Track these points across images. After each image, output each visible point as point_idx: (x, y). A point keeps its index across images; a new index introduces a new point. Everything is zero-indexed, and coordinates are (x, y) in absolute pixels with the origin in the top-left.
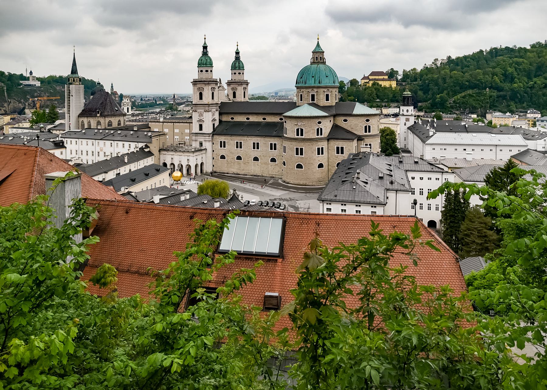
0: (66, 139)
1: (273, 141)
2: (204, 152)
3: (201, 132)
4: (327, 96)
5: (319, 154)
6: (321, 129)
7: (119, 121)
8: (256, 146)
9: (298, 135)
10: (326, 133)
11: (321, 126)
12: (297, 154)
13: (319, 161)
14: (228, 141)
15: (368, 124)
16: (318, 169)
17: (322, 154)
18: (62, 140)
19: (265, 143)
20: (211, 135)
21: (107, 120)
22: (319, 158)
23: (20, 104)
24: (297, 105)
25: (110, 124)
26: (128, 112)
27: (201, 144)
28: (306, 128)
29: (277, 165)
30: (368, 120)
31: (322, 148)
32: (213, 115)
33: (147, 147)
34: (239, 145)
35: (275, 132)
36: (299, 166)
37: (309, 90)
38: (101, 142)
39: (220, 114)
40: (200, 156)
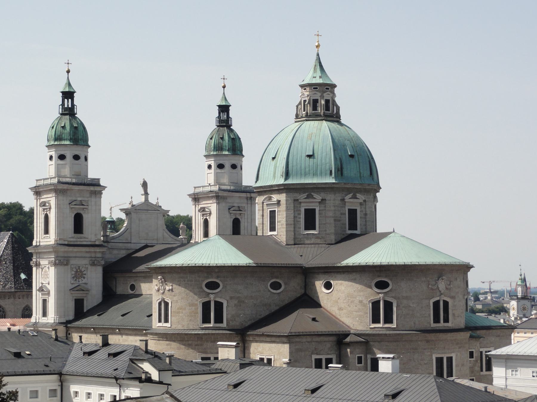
4: (310, 215)
28: (175, 298)
32: (79, 274)
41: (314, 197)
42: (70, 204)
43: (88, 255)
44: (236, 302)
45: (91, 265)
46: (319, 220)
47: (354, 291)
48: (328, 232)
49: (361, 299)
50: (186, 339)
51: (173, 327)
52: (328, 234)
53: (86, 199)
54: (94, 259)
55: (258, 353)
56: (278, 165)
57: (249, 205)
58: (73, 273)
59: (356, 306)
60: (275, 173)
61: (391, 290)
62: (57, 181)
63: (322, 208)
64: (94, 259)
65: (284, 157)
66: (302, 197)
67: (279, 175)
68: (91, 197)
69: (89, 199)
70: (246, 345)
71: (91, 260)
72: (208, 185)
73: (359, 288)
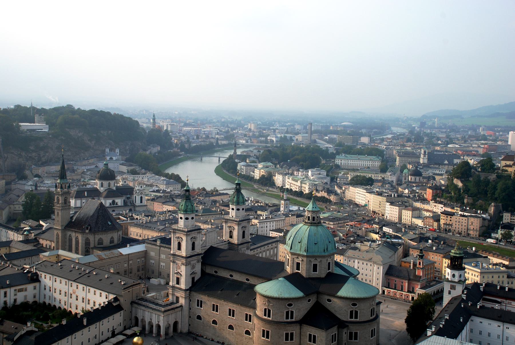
0: (41, 273)
2: (180, 309)
3: (177, 286)
5: (287, 339)
6: (292, 312)
7: (112, 238)
8: (232, 313)
9: (265, 315)
10: (298, 315)
11: (290, 309)
12: (263, 336)
15: (354, 308)
17: (292, 339)
18: (36, 273)
19: (241, 311)
20: (188, 291)
21: (98, 237)
23: (21, 160)
25: (100, 242)
26: (141, 202)
30: (354, 305)
31: (292, 334)
32: (193, 267)
33: (116, 299)
34: (215, 308)
35: (253, 301)
38: (75, 284)
39: (203, 264)
40: (173, 315)
42: (191, 239)
44: (298, 310)
45: (197, 262)
51: (273, 320)
56: (302, 246)
60: (301, 249)
61: (358, 307)
63: (320, 264)
66: (312, 260)
67: (303, 250)
68: (198, 234)
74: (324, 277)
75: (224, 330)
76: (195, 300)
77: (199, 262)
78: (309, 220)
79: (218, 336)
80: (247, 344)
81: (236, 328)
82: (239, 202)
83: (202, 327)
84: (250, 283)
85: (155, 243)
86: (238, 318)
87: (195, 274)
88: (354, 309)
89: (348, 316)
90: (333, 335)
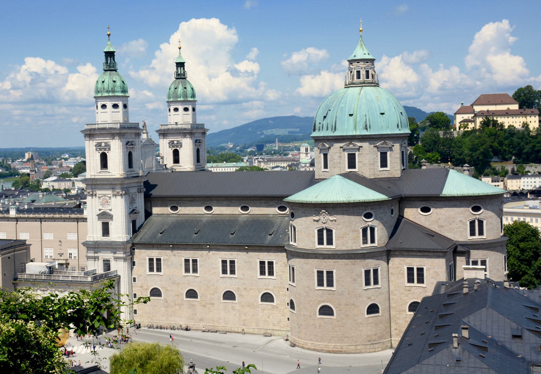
1: (266, 257)
3: (106, 239)
5: (368, 283)
9: (321, 242)
12: (320, 283)
13: (369, 298)
14: (166, 258)
16: (367, 316)
17: (376, 282)
22: (369, 293)
24: (316, 177)
27: (107, 265)
28: (339, 227)
29: (277, 308)
31: (376, 271)
36: (326, 311)
37: (342, 145)
41: (387, 144)
43: (136, 185)
45: (138, 192)
46: (390, 160)
47: (455, 214)
48: (396, 169)
49: (461, 219)
50: (353, 257)
51: (338, 248)
52: (397, 170)
53: (133, 140)
54: (139, 187)
55: (406, 263)
56: (358, 119)
57: (203, 138)
58: (130, 200)
59: (457, 224)
62: (119, 126)
64: (139, 187)
65: (364, 114)
67: (361, 128)
69: (135, 139)
70: (389, 258)
71: (138, 189)
72: (175, 123)
73: (459, 212)
74: (400, 176)
75: (213, 304)
76: (145, 259)
77: (141, 192)
78: (359, 77)
79: (201, 320)
80: (268, 319)
81: (241, 295)
82: (186, 96)
83: (163, 309)
84: (251, 213)
85: (6, 215)
86: (243, 275)
87: (136, 213)
88: (477, 216)
89: (466, 232)
90: (450, 265)
